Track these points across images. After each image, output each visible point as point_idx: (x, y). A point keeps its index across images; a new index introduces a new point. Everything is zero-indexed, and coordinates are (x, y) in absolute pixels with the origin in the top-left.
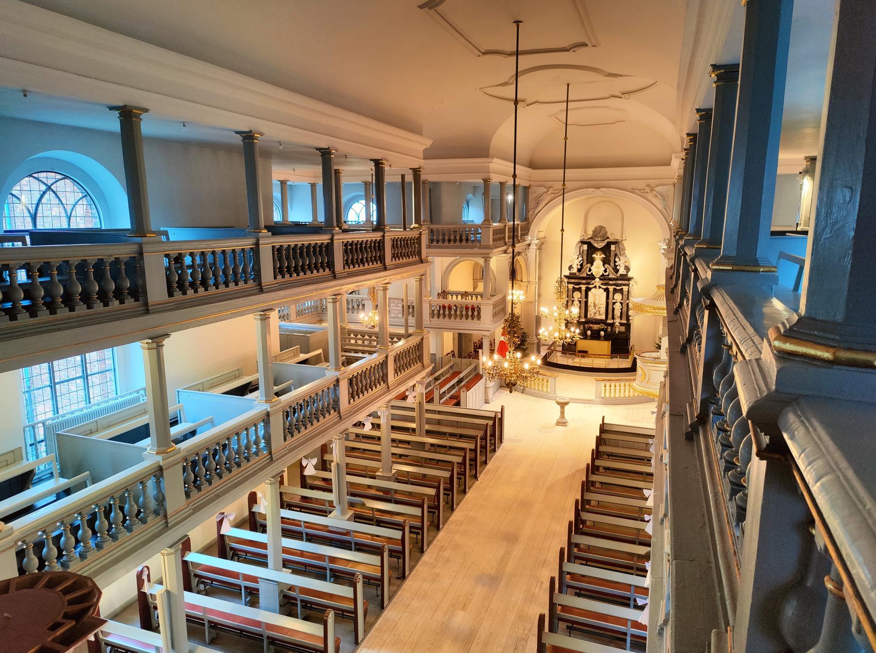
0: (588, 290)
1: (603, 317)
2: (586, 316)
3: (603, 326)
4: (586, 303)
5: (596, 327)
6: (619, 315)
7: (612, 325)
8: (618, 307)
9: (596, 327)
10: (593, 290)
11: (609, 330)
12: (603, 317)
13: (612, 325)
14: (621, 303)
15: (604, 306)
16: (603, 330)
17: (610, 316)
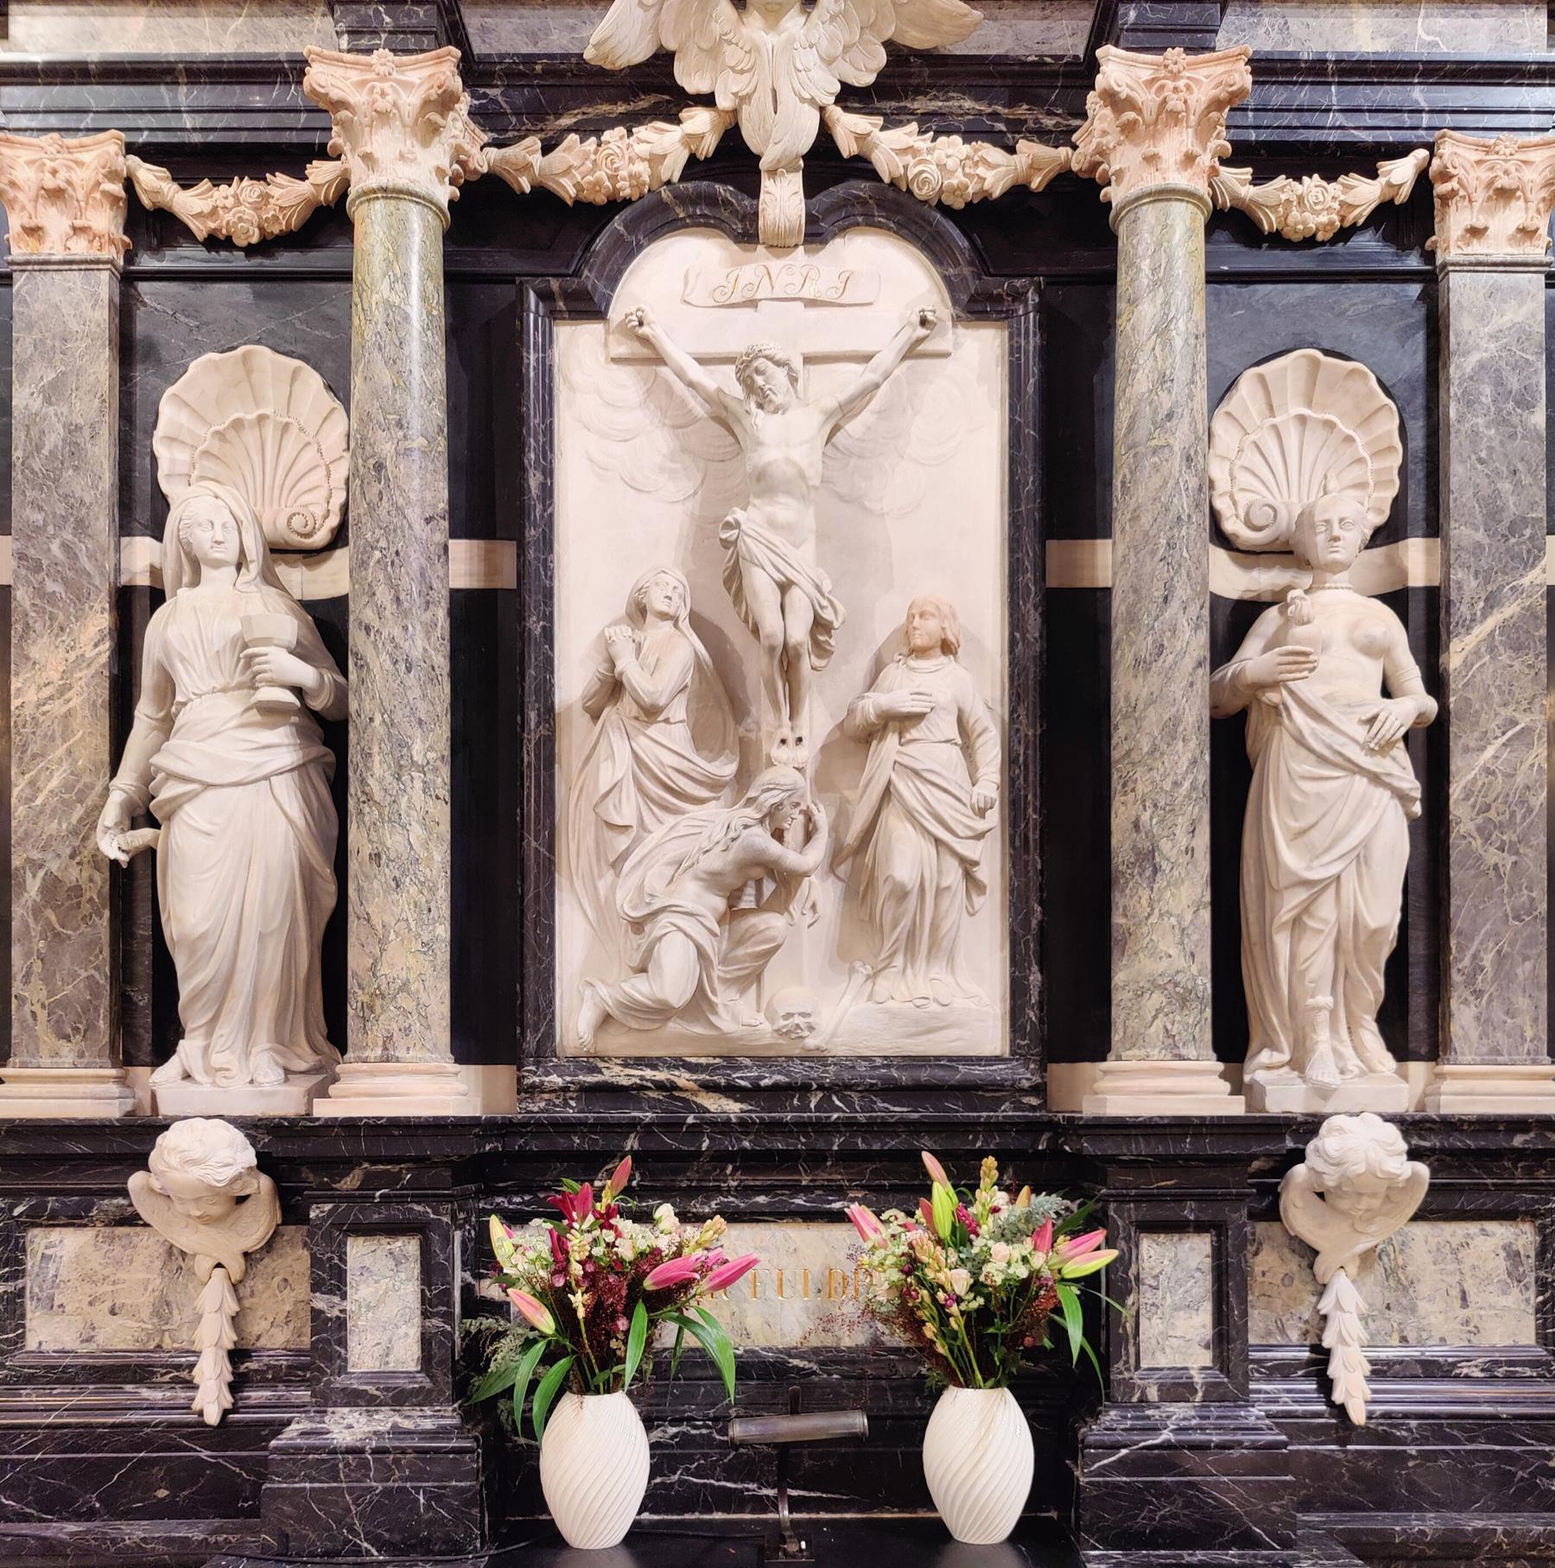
0: (521, 258)
1: (958, 1000)
2: (496, 995)
3: (1011, 1238)
4: (496, 646)
5: (788, 1285)
6: (1383, 910)
7: (1233, 1176)
8: (1340, 660)
9: (788, 1285)
10: (672, 278)
11: (1172, 1324)
12: (958, 1000)
13: (1233, 1176)
14: (1426, 616)
15: (969, 688)
16: (1017, 1343)
17: (1161, 936)
